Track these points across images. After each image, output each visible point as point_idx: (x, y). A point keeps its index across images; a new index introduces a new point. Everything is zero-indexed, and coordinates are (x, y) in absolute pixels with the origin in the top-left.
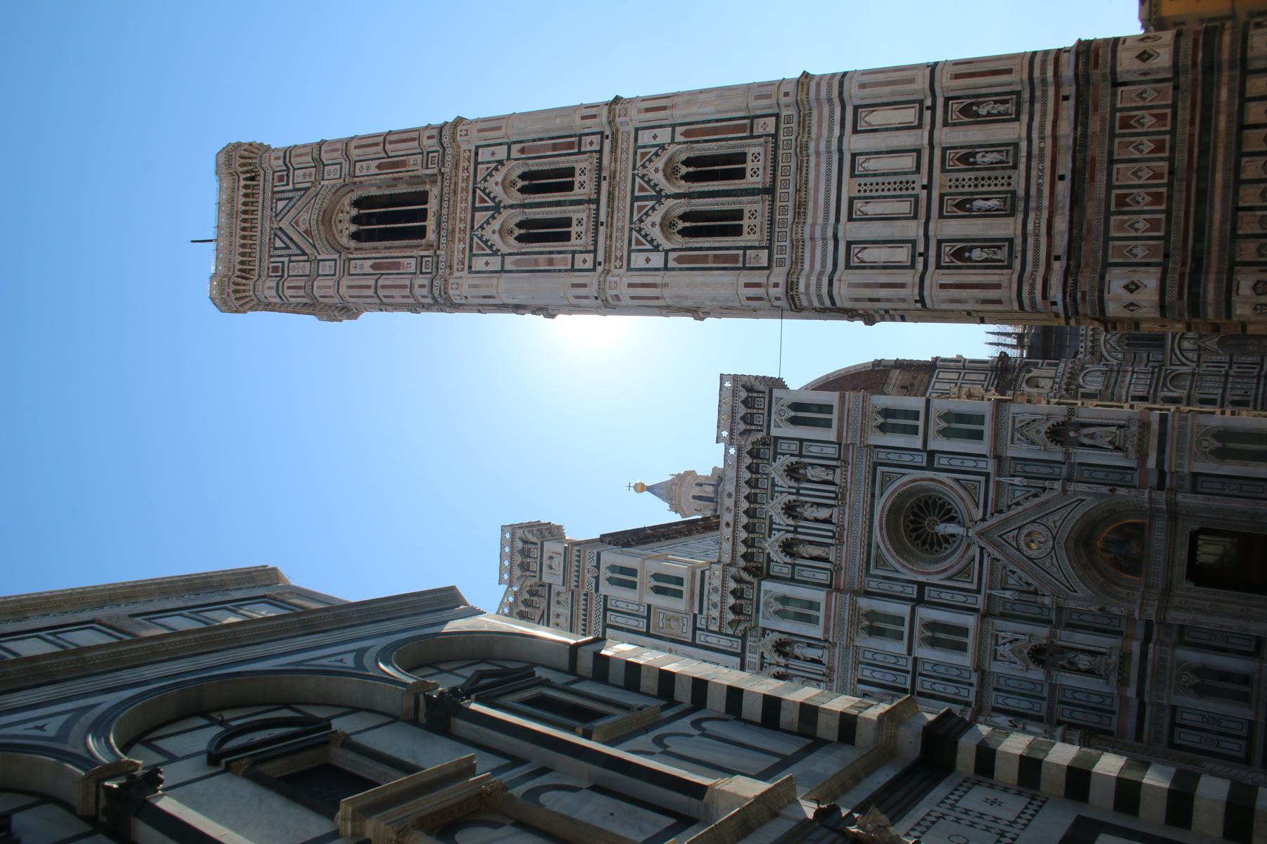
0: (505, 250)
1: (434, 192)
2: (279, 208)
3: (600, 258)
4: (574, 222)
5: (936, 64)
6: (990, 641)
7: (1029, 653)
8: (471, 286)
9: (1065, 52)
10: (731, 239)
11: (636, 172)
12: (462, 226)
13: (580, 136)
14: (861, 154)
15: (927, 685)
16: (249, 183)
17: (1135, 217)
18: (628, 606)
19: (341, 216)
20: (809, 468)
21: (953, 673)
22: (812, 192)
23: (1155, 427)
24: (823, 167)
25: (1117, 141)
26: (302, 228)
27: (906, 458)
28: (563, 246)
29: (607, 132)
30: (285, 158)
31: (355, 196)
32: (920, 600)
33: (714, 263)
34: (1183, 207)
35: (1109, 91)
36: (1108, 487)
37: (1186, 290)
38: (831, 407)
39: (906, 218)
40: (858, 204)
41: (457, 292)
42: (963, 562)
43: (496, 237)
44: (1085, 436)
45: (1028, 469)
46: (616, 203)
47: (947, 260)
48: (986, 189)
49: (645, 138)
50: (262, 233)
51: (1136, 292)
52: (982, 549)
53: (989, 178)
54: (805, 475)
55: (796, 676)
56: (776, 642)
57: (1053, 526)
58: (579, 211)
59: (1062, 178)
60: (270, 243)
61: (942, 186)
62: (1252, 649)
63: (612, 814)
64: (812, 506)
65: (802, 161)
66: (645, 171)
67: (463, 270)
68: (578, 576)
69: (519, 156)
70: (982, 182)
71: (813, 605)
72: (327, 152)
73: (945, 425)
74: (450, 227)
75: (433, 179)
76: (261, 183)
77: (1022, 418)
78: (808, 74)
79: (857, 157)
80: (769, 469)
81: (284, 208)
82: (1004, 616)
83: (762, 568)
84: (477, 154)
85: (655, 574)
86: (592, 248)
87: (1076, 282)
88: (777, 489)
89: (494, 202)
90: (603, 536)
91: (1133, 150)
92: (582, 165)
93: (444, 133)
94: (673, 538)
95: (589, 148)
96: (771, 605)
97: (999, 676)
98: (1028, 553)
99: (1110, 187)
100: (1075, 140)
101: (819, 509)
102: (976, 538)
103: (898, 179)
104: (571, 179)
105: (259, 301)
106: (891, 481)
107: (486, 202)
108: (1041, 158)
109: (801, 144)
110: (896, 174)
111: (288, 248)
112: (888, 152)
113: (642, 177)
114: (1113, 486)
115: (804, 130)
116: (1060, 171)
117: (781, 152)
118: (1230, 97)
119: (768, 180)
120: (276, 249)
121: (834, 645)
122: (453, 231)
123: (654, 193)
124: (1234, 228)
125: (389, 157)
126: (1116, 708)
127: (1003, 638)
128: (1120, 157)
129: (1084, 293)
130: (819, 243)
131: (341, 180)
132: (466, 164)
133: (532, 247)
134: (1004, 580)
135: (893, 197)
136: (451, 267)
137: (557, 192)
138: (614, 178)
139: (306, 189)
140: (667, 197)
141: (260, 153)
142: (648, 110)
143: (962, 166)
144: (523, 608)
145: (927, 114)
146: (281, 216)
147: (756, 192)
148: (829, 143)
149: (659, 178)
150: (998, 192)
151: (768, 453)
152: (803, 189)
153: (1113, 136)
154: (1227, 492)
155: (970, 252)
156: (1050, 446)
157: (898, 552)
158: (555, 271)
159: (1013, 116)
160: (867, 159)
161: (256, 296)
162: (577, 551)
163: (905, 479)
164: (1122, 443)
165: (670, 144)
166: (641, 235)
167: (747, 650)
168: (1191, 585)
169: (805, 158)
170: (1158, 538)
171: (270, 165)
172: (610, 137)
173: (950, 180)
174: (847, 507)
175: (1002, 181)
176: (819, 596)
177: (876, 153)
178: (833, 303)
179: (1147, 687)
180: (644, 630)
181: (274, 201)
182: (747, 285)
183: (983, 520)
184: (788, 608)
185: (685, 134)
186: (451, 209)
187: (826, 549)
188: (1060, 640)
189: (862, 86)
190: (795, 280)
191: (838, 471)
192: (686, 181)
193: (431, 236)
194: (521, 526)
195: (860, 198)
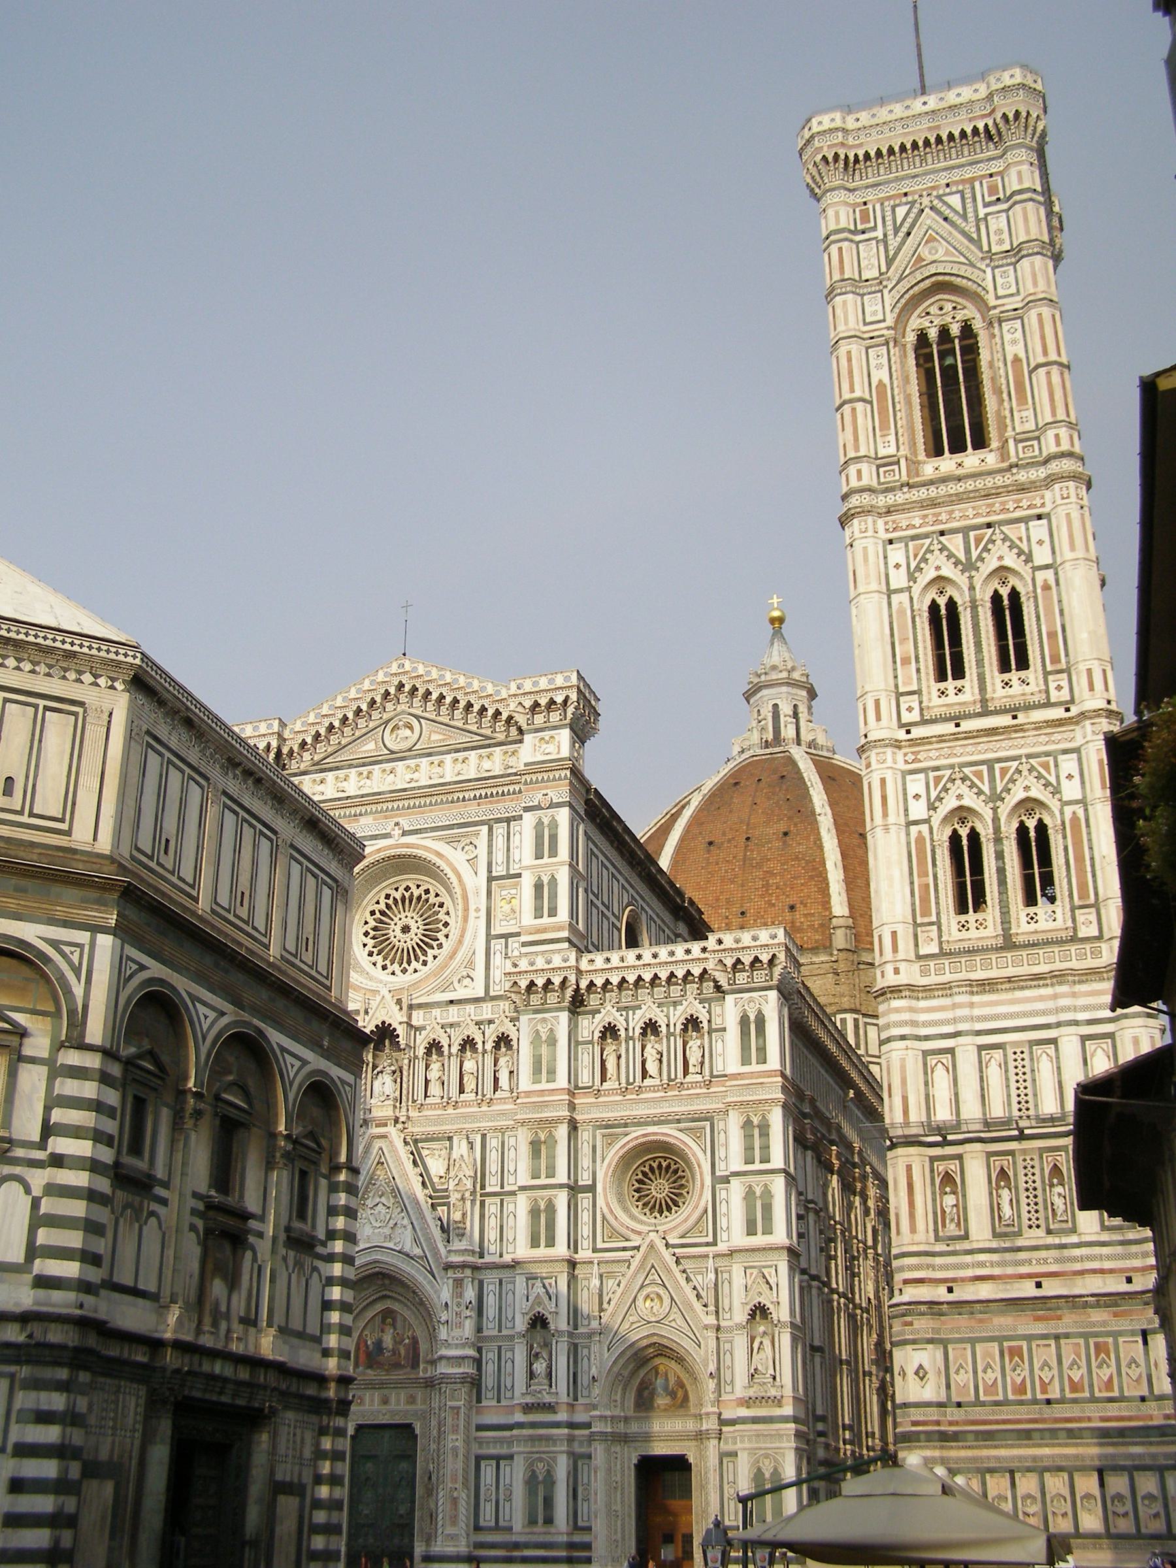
0: (916, 590)
12: (944, 517)
13: (1068, 671)
14: (1057, 1050)
15: (493, 1209)
17: (998, 1368)
19: (948, 307)
20: (699, 1042)
21: (508, 1234)
23: (777, 1412)
24: (1040, 1006)
25: (1081, 1341)
26: (924, 252)
27: (720, 1153)
28: (927, 674)
29: (1075, 711)
30: (1020, 192)
31: (978, 325)
32: (574, 1189)
40: (998, 1055)
42: (624, 1231)
43: (933, 574)
45: (726, 1283)
46: (985, 739)
47: (941, 1168)
48: (1024, 1201)
49: (1068, 764)
52: (637, 1248)
59: (1039, 1285)
60: (898, 196)
61: (1024, 1151)
62: (580, 1523)
65: (1045, 978)
69: (1039, 583)
71: (552, 1072)
73: (758, 1194)
81: (950, 207)
84: (1039, 517)
87: (923, 1314)
89: (976, 561)
95: (1052, 686)
98: (640, 1298)
99: (1029, 1338)
102: (647, 1241)
104: (1013, 667)
108: (1058, 1261)
110: (1035, 1095)
111: (896, 231)
112: (1060, 1083)
116: (1045, 1282)
118: (1131, 1456)
120: (893, 208)
124: (991, 1471)
125: (1030, 373)
126: (504, 1403)
129: (911, 1324)
133: (923, 629)
134: (611, 1275)
135: (1009, 1096)
138: (1016, 731)
139: (977, 243)
140: (995, 809)
143: (1047, 1172)
147: (1006, 926)
149: (1018, 794)
150: (1019, 1216)
152: (1011, 985)
153: (1086, 1336)
154: (726, 1486)
158: (895, 670)
163: (700, 1154)
167: (494, 1003)
168: (635, 1461)
169: (1049, 981)
175: (1034, 1219)
176: (562, 1081)
177: (1059, 1068)
180: (494, 874)
181: (960, 188)
182: (894, 934)
190: (903, 994)
191: (699, 1078)
192: (1017, 829)
193: (930, 468)
195: (1005, 1055)
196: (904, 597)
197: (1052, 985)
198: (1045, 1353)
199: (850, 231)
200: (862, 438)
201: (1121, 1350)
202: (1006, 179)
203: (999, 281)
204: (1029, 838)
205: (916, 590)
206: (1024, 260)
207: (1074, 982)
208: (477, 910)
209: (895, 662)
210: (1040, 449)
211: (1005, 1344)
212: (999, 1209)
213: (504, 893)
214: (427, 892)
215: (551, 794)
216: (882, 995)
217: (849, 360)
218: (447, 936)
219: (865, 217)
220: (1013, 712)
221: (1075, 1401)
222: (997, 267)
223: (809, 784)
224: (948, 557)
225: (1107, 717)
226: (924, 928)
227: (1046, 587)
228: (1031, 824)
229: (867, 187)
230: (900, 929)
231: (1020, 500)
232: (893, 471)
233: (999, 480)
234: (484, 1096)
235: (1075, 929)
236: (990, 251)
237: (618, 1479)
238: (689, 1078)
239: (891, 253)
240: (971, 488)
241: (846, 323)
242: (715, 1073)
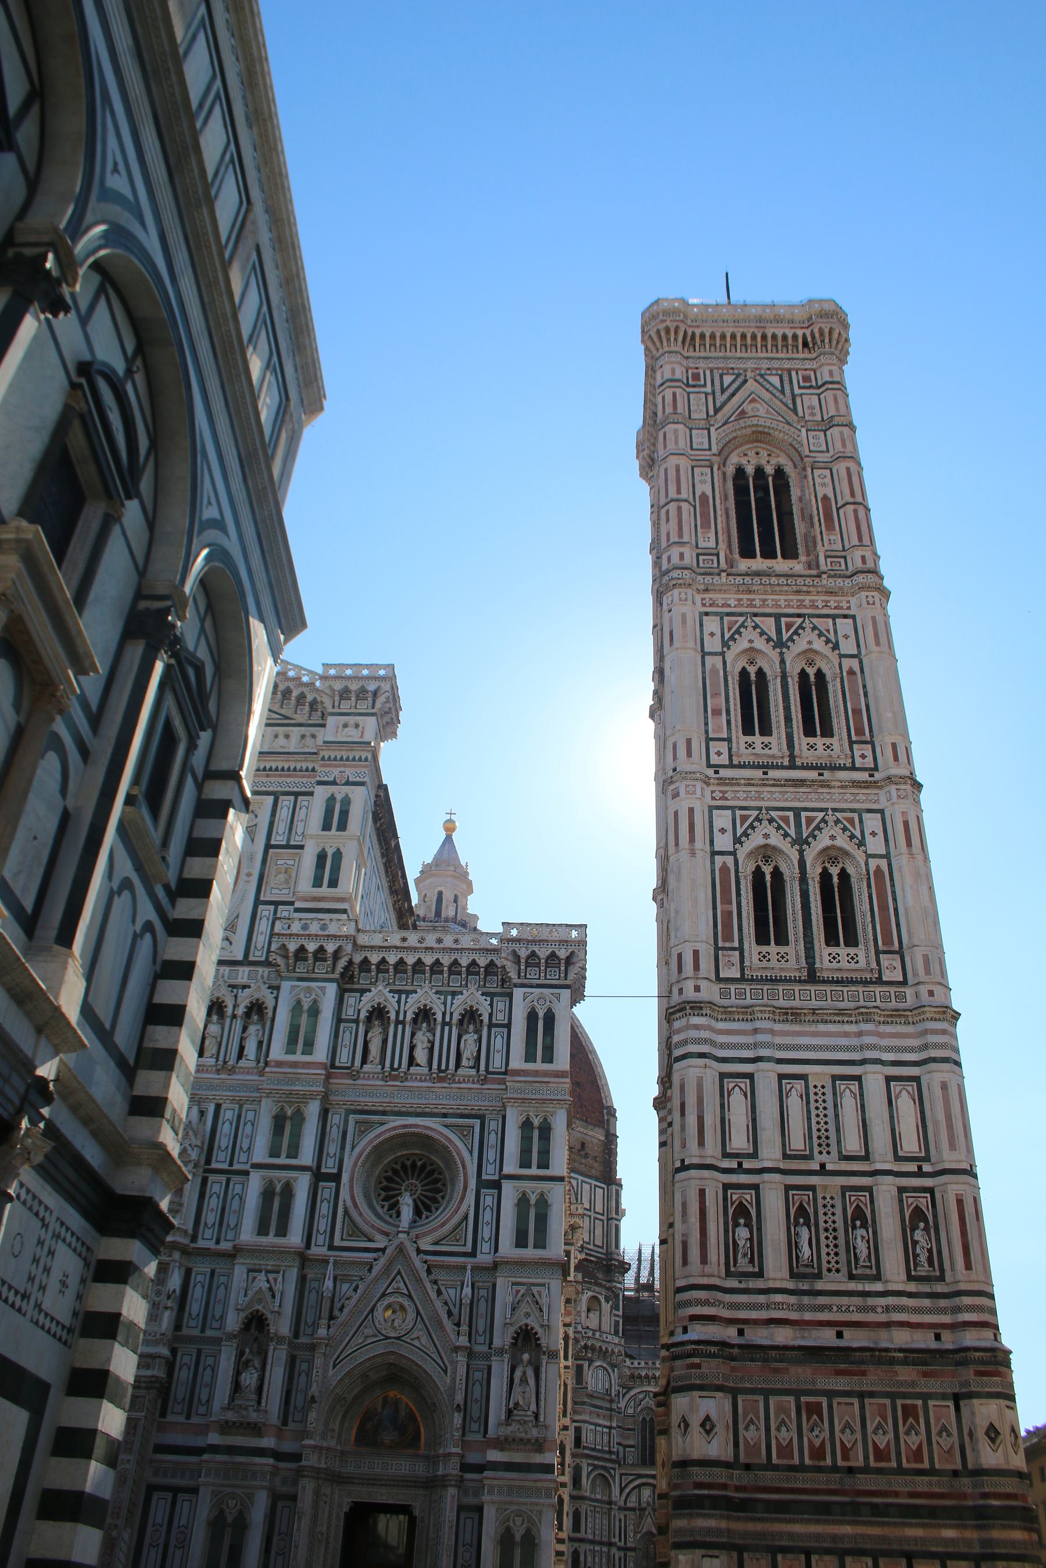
0: (730, 656)
1: (797, 566)
3: (724, 773)
4: (766, 739)
5: (975, 1176)
6: (271, 1264)
7: (257, 1311)
8: (684, 616)
9: (995, 1335)
11: (830, 812)
12: (757, 603)
13: (872, 743)
14: (861, 1087)
15: (216, 1188)
17: (794, 1426)
18: (302, 821)
19: (764, 454)
20: (476, 1037)
22: (813, 1028)
23: (538, 1459)
25: (887, 1402)
26: (748, 407)
27: (491, 1155)
28: (736, 726)
29: (878, 776)
31: (789, 469)
32: (318, 1176)
33: (722, 912)
34: (808, 1486)
35: (949, 1391)
36: (462, 1403)
37: (706, 1492)
38: (551, 1061)
39: (784, 1145)
40: (799, 1085)
41: (676, 599)
44: (524, 1373)
45: (482, 1302)
46: (792, 789)
47: (735, 1197)
48: (823, 1242)
49: (872, 822)
50: (740, 358)
51: (701, 1430)
52: (383, 1250)
53: (836, 1246)
54: (467, 1032)
55: (223, 1029)
56: (263, 1003)
57: (413, 1336)
59: (840, 1335)
60: (728, 369)
61: (825, 1187)
63: (35, 838)
64: (429, 1041)
65: (850, 1015)
66: (831, 823)
67: (704, 605)
68: (335, 759)
69: (845, 669)
70: (831, 1237)
71: (309, 1046)
72: (842, 433)
73: (533, 1201)
74: (755, 588)
76: (801, 355)
77: (544, 1295)
78: (957, 1019)
80: (472, 988)
81: (769, 383)
82: (302, 1279)
83: (353, 983)
84: (845, 617)
86: (735, 762)
88: (449, 998)
89: (787, 641)
90: (385, 788)
91: (876, 1422)
92: (836, 746)
93: (870, 575)
94: (387, 872)
95: (857, 754)
96: (308, 995)
97: (229, 1276)
98: (380, 1308)
99: (830, 1394)
100: (887, 1350)
101: (426, 1051)
103: (832, 1134)
104: (819, 733)
105: (657, 359)
106: (463, 1137)
107: (787, 632)
110: (838, 1130)
111: (723, 391)
112: (864, 1121)
113: (823, 820)
114: (464, 1409)
115: (888, 1016)
116: (847, 1333)
117: (861, 989)
119: (825, 975)
120: (721, 376)
121: (261, 1073)
122: (750, 592)
123: (805, 836)
125: (838, 509)
126: (194, 1420)
127: (275, 1280)
128: (867, 1406)
129: (698, 1366)
130: (750, 1040)
131: (807, 453)
132: (832, 604)
134: (346, 1278)
135: (810, 1128)
136: (706, 590)
137: (803, 717)
138: (822, 786)
139: (795, 411)
140: (801, 852)
141: (837, 352)
142: (906, 824)
143: (849, 1212)
144: (295, 693)
145: (912, 1167)
146: (761, 380)
147: (810, 960)
148: (874, 1047)
149: (823, 841)
150: (819, 1257)
151: (493, 986)
152: (816, 1018)
153: (893, 1396)
154: (461, 1550)
155: (745, 1225)
156: (511, 1331)
157: (376, 1147)
158: (706, 718)
159: (913, 1273)
160: (855, 1095)
161: (663, 355)
163: (465, 1154)
164: (517, 1418)
165: (865, 852)
166: (754, 821)
167: (252, 968)
168: (346, 1508)
169: (853, 1019)
170: (402, 1466)
171: (822, 365)
172: (871, 779)
173: (832, 1198)
174: (430, 1084)
175: (833, 1261)
176: (321, 1053)
177: (863, 1106)
178: (678, 1059)
179: (219, 1458)
180: (273, 842)
181: (780, 372)
182: (696, 953)
183: (419, 1251)
184: (305, 1016)
185: (878, 871)
186: (777, 588)
187: (377, 1061)
188: (274, 1349)
189: (944, 1086)
190: (704, 1012)
191: (473, 1072)
193: (744, 565)
194: (394, 688)
195: (807, 1087)
198: (847, 1411)
200: (685, 529)
201: (931, 1414)
208: (249, 875)
211: (802, 1399)
212: (797, 1247)
216: (680, 1011)
220: (819, 768)
221: (880, 1471)
228: (834, 871)
235: (880, 972)
237: (324, 1529)
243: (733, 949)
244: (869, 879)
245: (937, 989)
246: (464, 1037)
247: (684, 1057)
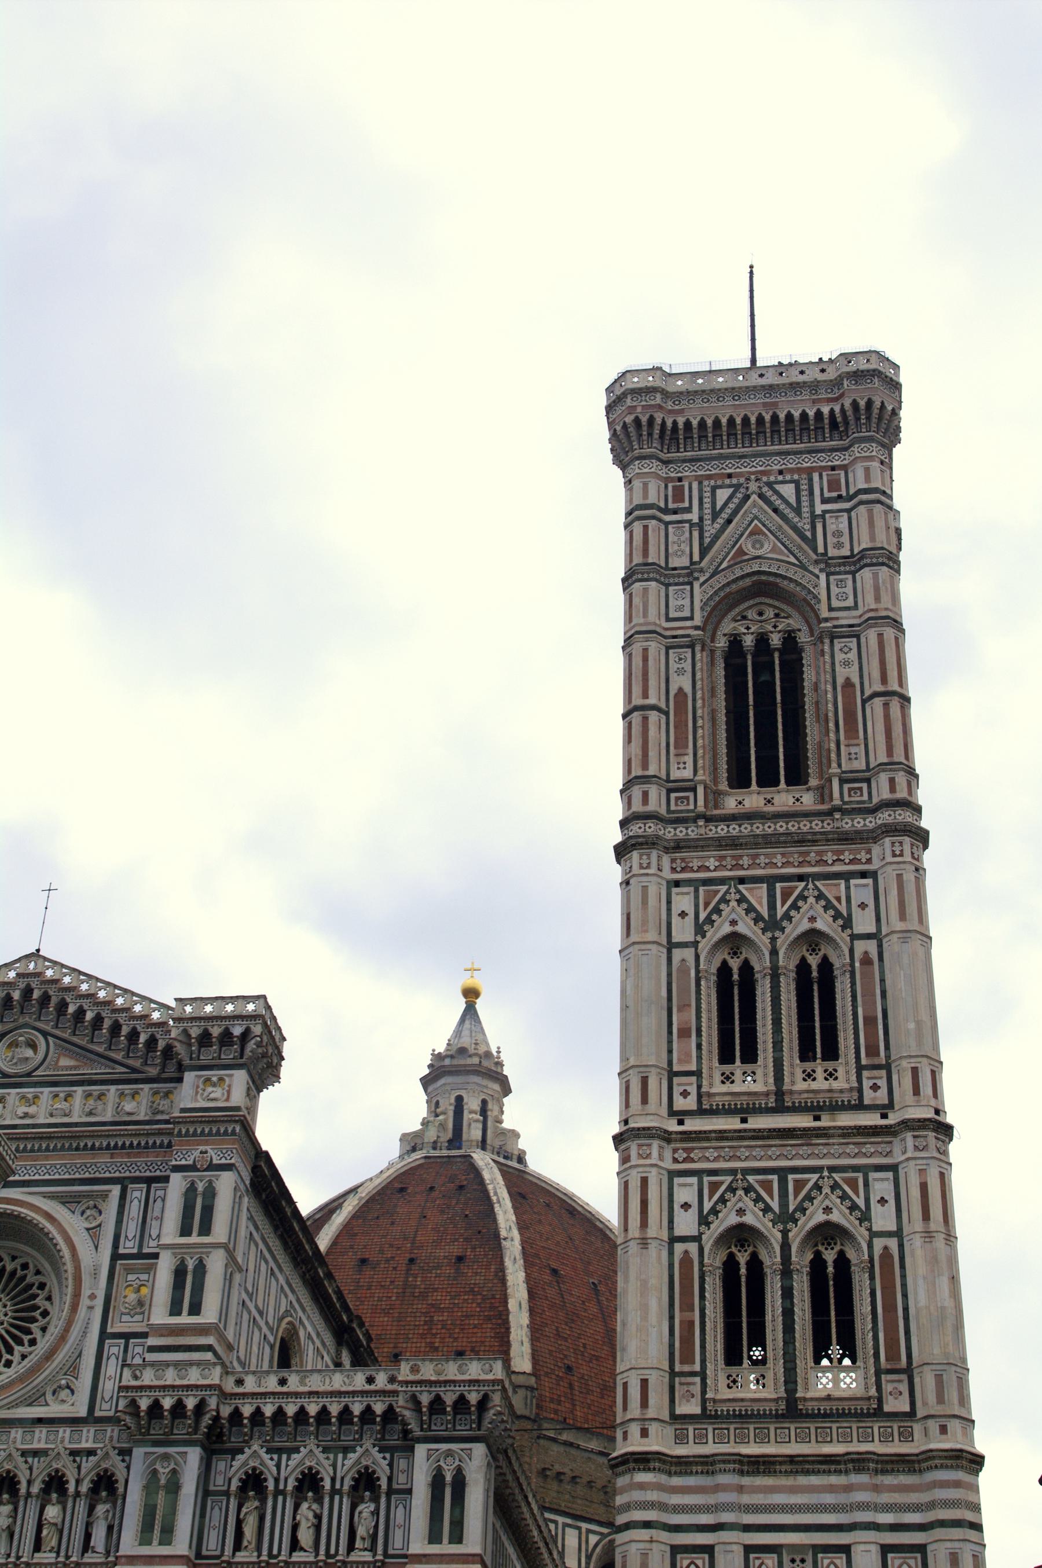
0: (705, 946)
2: (780, 488)
10: (720, 1347)
13: (887, 1067)
16: (826, 421)
18: (157, 1218)
19: (770, 613)
20: (372, 1507)
24: (829, 1499)
28: (710, 1052)
30: (866, 491)
31: (803, 638)
33: (681, 1322)
38: (460, 1541)
43: (727, 929)
46: (777, 1142)
49: (882, 1186)
54: (362, 1501)
58: (765, 1075)
65: (838, 1463)
66: (826, 1190)
69: (858, 955)
71: (168, 1535)
75: (823, 793)
79: (844, 1556)
80: (368, 1444)
83: (223, 1442)
84: (863, 875)
85: (205, 1266)
88: (340, 1456)
89: (782, 919)
92: (841, 1073)
95: (867, 1084)
96: (165, 1464)
101: (311, 1531)
104: (819, 1055)
107: (783, 905)
109: (864, 1460)
111: (715, 515)
113: (818, 1187)
115: (887, 1462)
119: (810, 1405)
123: (791, 1208)
125: (864, 702)
133: (709, 995)
138: (818, 1136)
139: (812, 543)
140: (785, 1233)
142: (924, 1187)
146: (769, 493)
147: (791, 1386)
151: (394, 1439)
152: (794, 1467)
158: (670, 1042)
161: (632, 461)
162: (234, 1129)
165: (869, 1230)
169: (842, 1467)
176: (181, 1545)
180: (121, 1251)
181: (796, 477)
182: (644, 1383)
184: (161, 1494)
187: (253, 1545)
190: (652, 1465)
192: (811, 1262)
196: (689, 954)
197: (847, 1472)
199: (660, 509)
200: (652, 754)
202: (850, 475)
203: (835, 590)
204: (826, 1276)
205: (705, 946)
206: (867, 569)
207: (876, 1472)
208: (92, 1297)
209: (670, 1032)
210: (870, 794)
213: (130, 1277)
214: (25, 1266)
215: (211, 1152)
217: (645, 659)
218: (44, 1329)
219: (678, 495)
220: (815, 1110)
222: (833, 574)
223: (494, 1199)
224: (748, 911)
225: (934, 1130)
226: (684, 1380)
227: (866, 961)
228: (830, 1256)
229: (684, 461)
230: (653, 1378)
231: (842, 852)
232: (687, 798)
233: (817, 825)
234: (67, 1557)
235: (880, 1400)
236: (826, 553)
238: (354, 1557)
239: (707, 540)
240: (781, 830)
241: (645, 615)
242: (391, 1552)
243: (693, 1374)
244: (873, 1266)
245: (954, 1425)
246: (359, 1508)
247: (628, 1526)
